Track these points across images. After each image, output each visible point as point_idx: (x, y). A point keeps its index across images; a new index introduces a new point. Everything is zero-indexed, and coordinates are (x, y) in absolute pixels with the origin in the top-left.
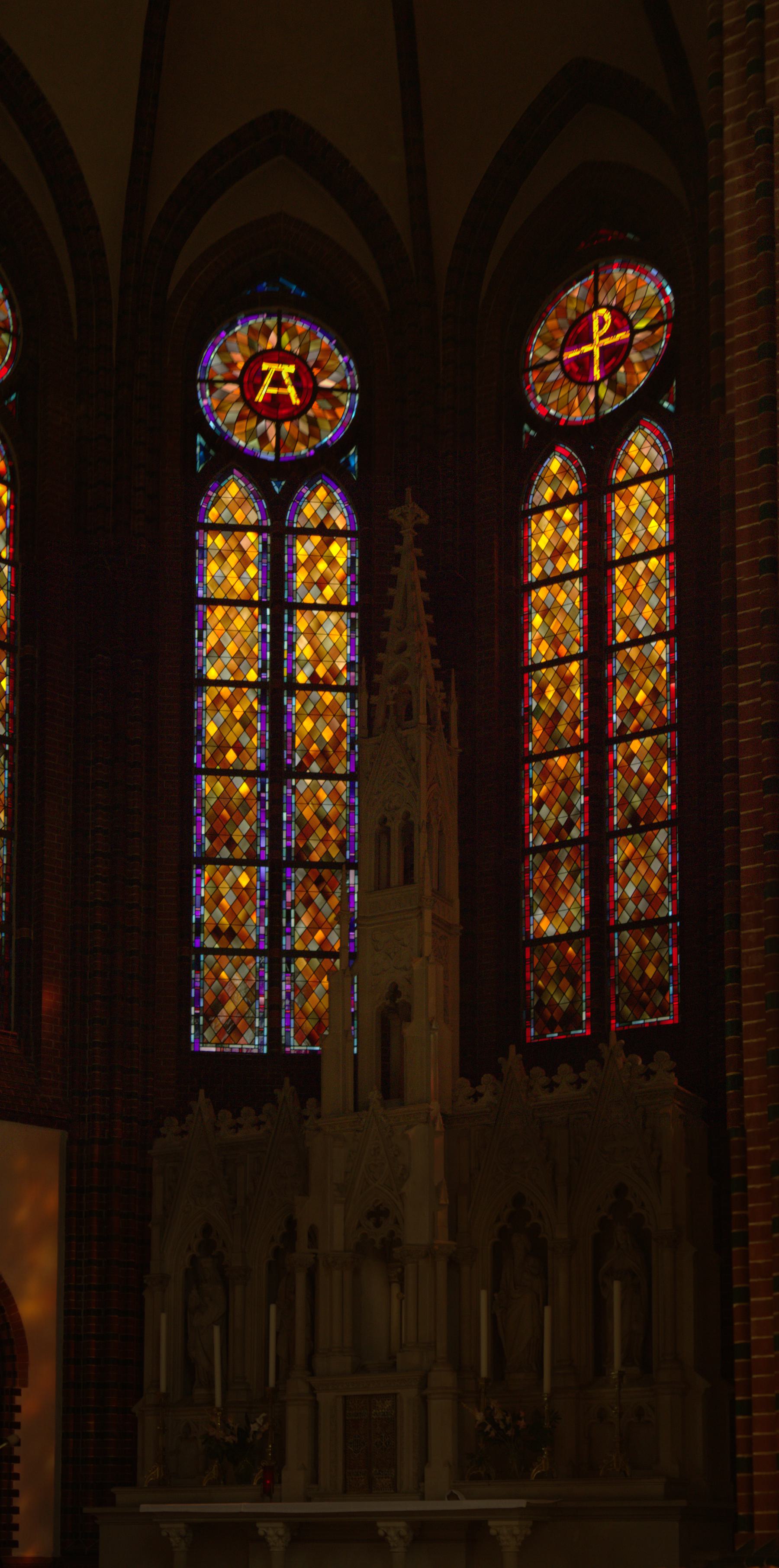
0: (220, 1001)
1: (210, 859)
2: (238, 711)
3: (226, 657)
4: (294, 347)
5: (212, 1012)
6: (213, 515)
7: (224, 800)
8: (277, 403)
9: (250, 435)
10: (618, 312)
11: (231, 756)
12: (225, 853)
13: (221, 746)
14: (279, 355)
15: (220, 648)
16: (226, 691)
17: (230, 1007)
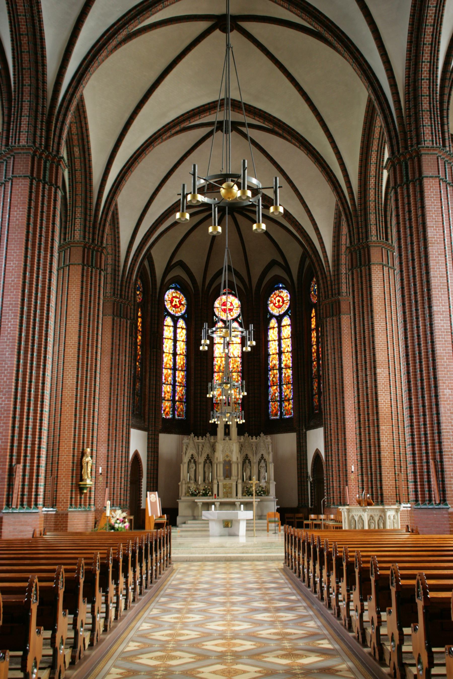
0: (165, 409)
1: (164, 384)
2: (169, 358)
3: (168, 348)
4: (178, 296)
5: (164, 411)
6: (165, 324)
7: (167, 373)
8: (176, 305)
9: (172, 310)
10: (231, 303)
11: (168, 366)
12: (167, 383)
13: (167, 364)
14: (176, 297)
15: (166, 347)
16: (167, 354)
17: (167, 410)
